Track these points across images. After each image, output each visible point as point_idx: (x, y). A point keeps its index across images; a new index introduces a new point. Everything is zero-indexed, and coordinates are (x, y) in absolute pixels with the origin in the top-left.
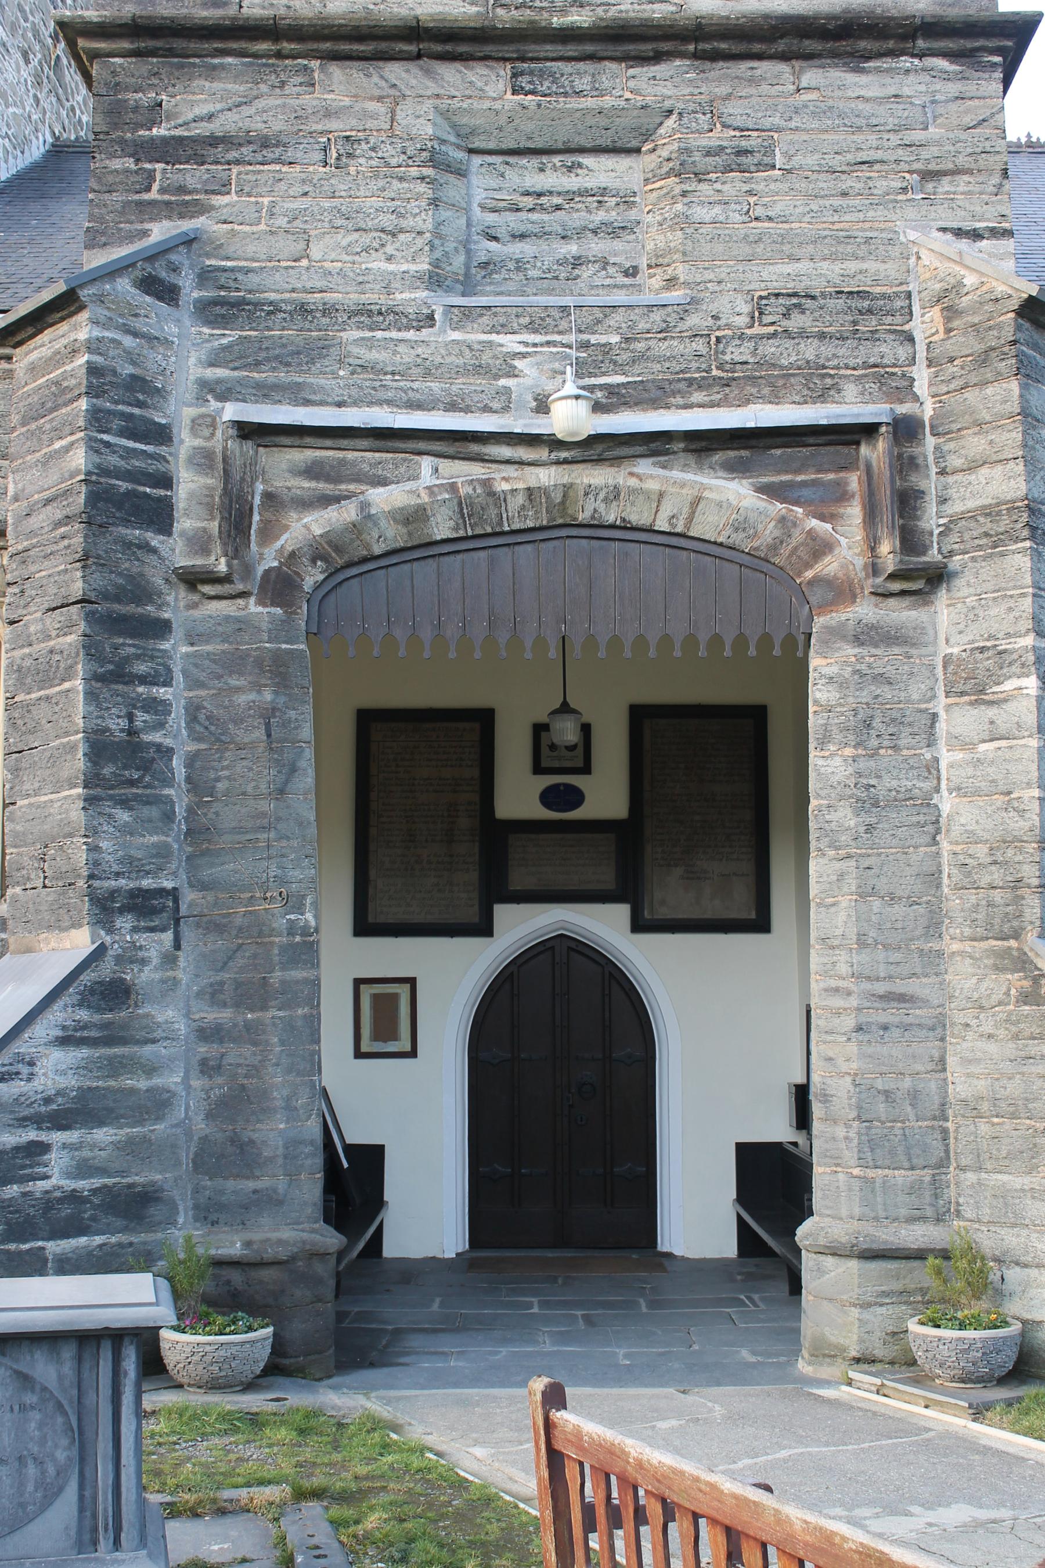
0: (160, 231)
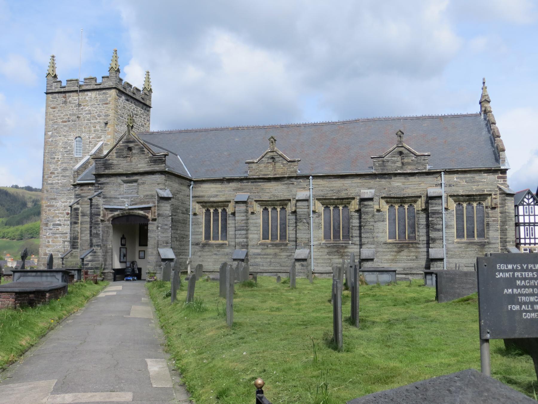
0: (100, 191)
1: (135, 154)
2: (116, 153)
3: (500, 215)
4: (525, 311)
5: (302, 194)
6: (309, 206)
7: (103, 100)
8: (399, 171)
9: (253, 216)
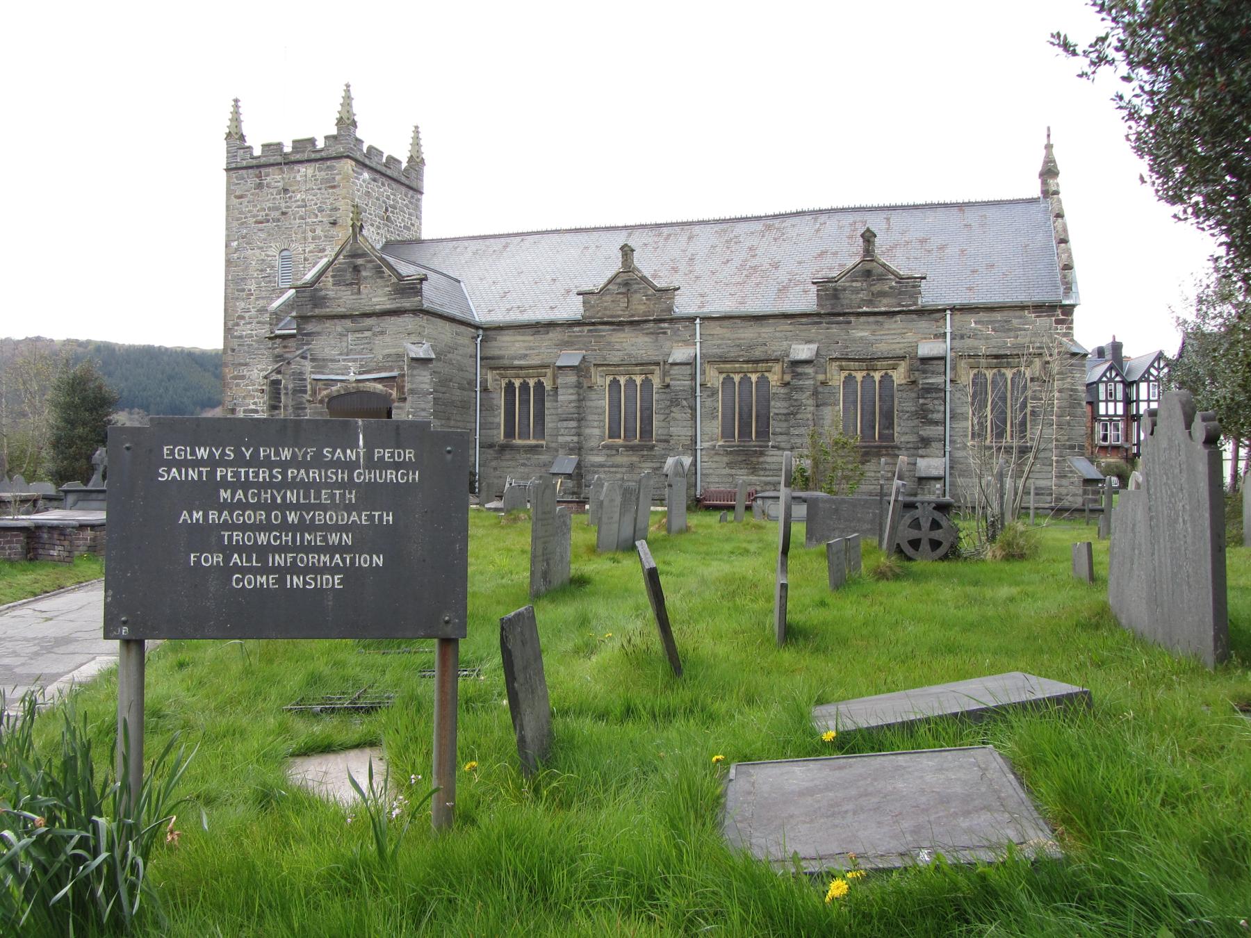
1: (365, 278)
2: (333, 276)
3: (1056, 394)
4: (237, 569)
5: (680, 354)
6: (694, 378)
7: (328, 181)
8: (865, 309)
9: (593, 395)
